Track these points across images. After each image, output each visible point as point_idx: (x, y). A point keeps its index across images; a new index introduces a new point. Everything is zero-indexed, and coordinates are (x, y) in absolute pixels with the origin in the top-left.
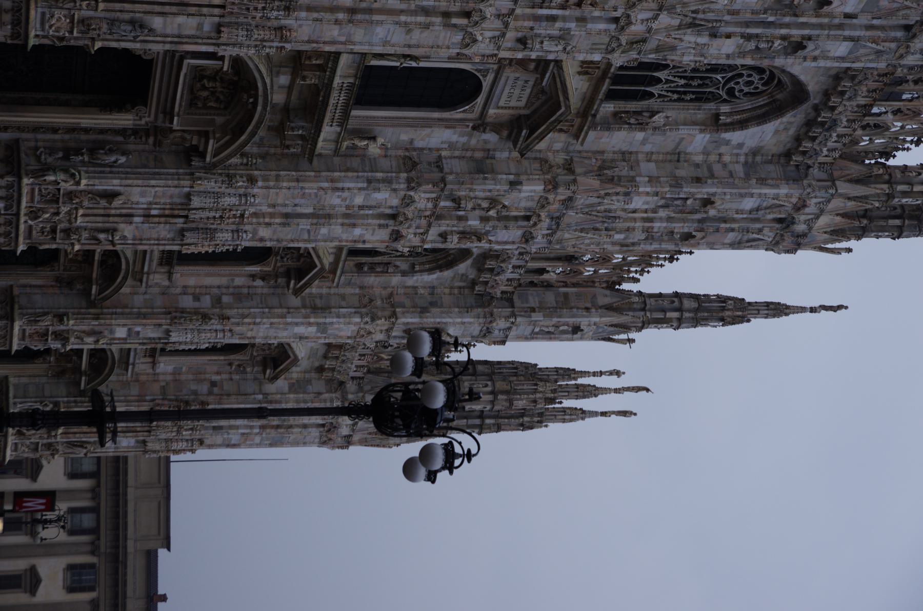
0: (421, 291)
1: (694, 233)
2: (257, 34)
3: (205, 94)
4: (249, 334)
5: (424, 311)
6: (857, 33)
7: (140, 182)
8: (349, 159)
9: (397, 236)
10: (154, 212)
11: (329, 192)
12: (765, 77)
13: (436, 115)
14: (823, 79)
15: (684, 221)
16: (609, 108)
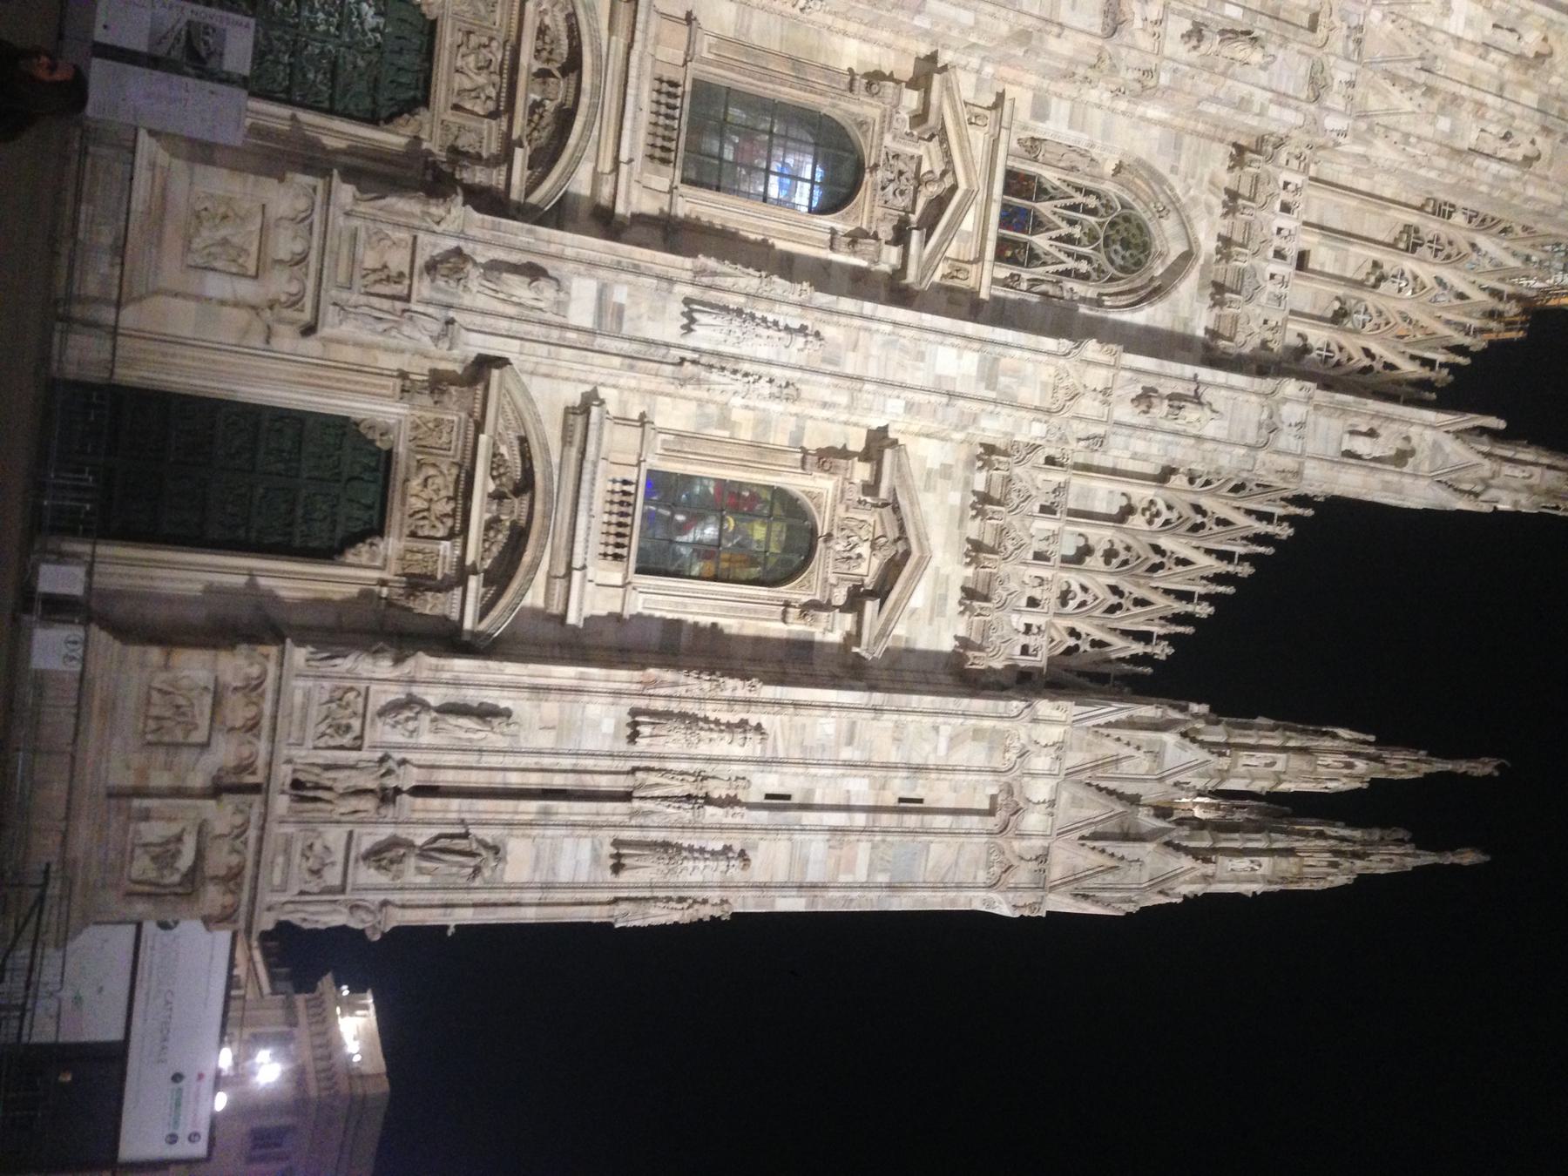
4: (851, 365)
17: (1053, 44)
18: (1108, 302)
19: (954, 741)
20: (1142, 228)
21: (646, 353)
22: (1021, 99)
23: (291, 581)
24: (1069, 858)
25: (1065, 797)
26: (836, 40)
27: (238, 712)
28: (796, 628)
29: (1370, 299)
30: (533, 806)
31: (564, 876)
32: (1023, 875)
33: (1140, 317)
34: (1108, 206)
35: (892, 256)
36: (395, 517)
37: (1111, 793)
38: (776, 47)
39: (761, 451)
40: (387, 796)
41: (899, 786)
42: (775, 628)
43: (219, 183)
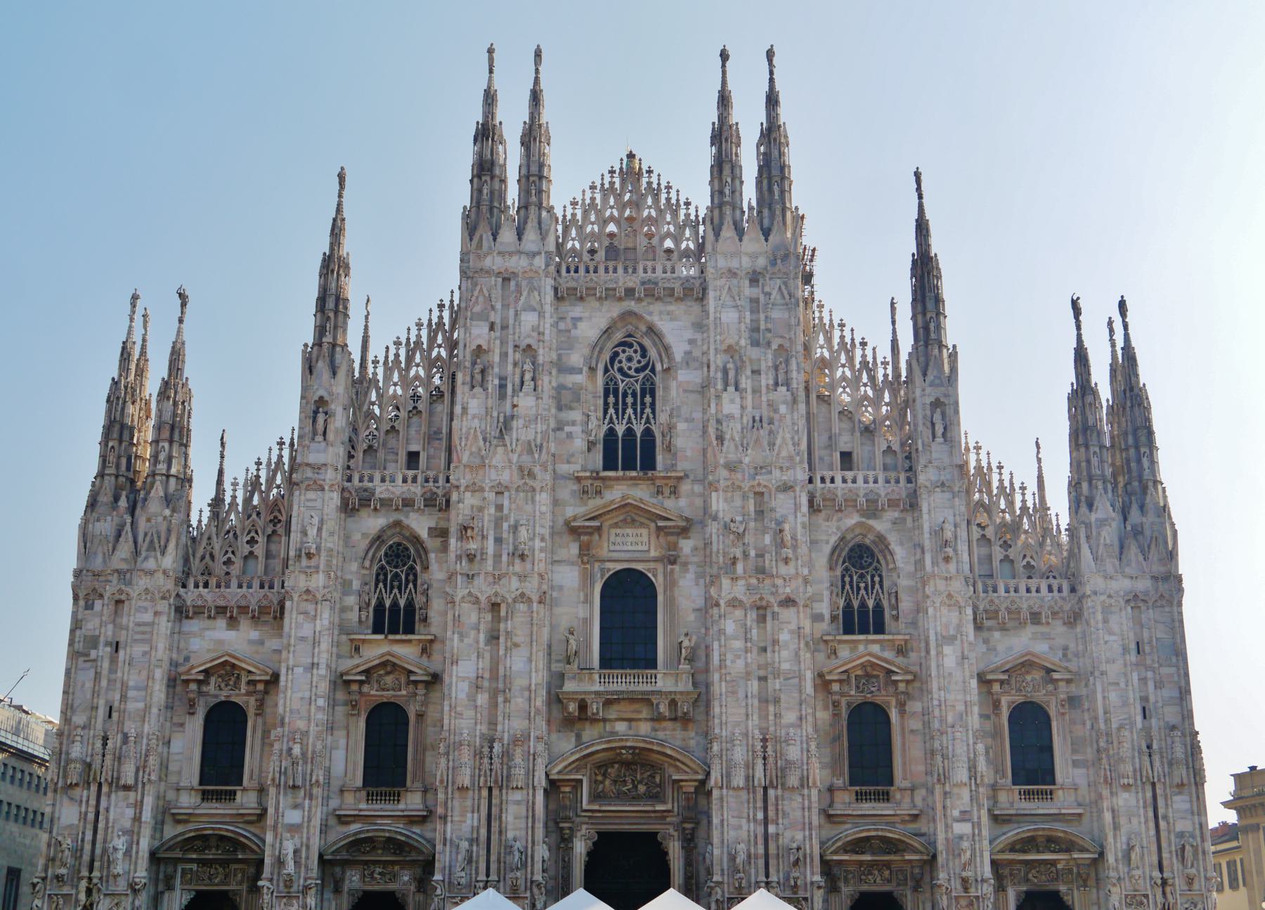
0: (918, 557)
1: (774, 346)
2: (518, 759)
3: (642, 788)
4: (960, 707)
5: (923, 552)
6: (512, 312)
7: (716, 835)
8: (707, 656)
9: (789, 602)
10: (760, 815)
11: (723, 671)
12: (620, 349)
13: (660, 598)
14: (604, 309)
15: (759, 360)
16: (659, 458)
17: (808, 630)
18: (891, 566)
19: (1111, 633)
20: (852, 550)
25: (1127, 570)
26: (819, 722)
30: (1162, 824)
31: (1187, 806)
32: (1163, 587)
34: (846, 570)
36: (1051, 887)
37: (1122, 547)
38: (828, 750)
39: (996, 734)
40: (1164, 882)
41: (1133, 657)
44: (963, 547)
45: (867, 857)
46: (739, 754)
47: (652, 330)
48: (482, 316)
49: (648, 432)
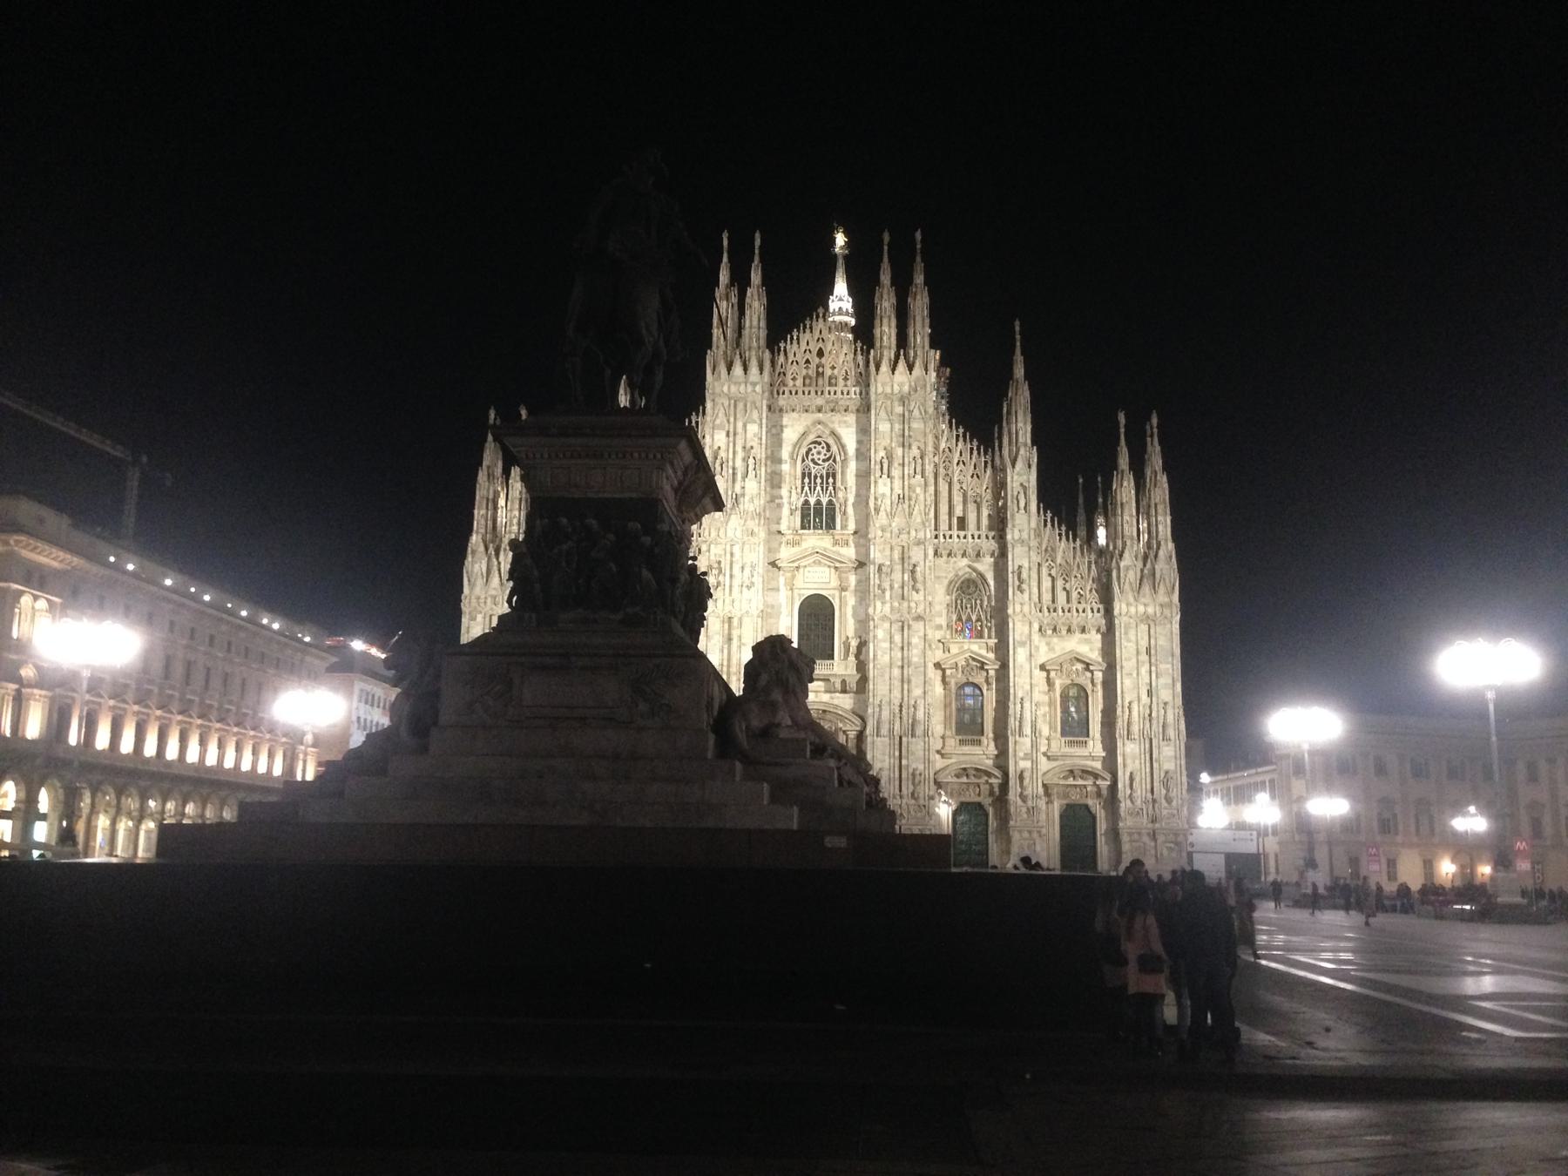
9: (919, 618)
17: (930, 636)
19: (1129, 641)
21: (1035, 745)
22: (939, 635)
23: (1102, 826)
24: (1162, 597)
27: (1136, 837)
28: (1099, 688)
29: (970, 493)
31: (1172, 754)
32: (1167, 612)
33: (992, 583)
35: (992, 673)
39: (1051, 703)
40: (1154, 801)
41: (1144, 657)
42: (1100, 694)
43: (1015, 849)
44: (1034, 584)
45: (964, 780)
46: (885, 714)
47: (833, 433)
48: (721, 427)
49: (830, 502)
